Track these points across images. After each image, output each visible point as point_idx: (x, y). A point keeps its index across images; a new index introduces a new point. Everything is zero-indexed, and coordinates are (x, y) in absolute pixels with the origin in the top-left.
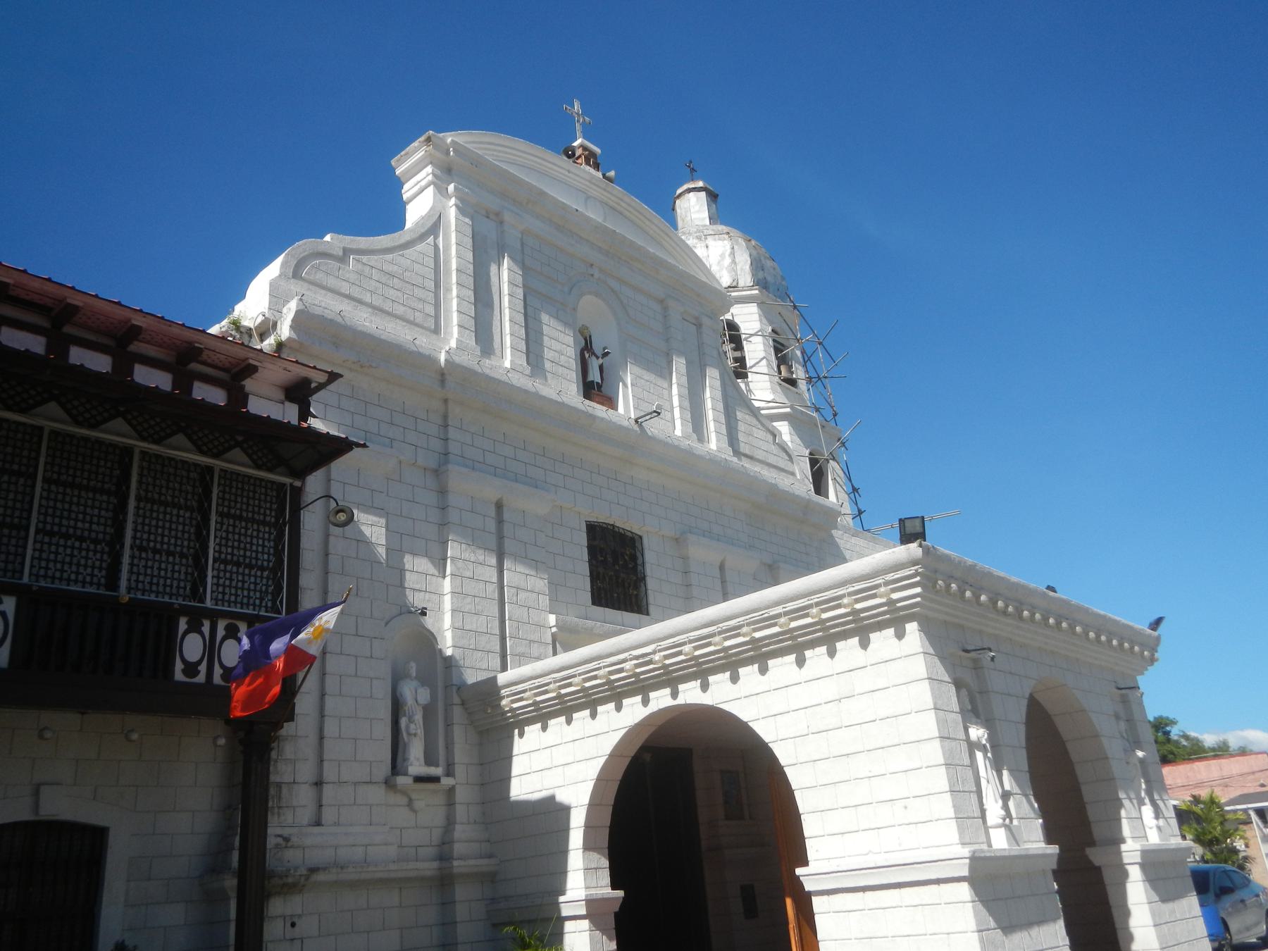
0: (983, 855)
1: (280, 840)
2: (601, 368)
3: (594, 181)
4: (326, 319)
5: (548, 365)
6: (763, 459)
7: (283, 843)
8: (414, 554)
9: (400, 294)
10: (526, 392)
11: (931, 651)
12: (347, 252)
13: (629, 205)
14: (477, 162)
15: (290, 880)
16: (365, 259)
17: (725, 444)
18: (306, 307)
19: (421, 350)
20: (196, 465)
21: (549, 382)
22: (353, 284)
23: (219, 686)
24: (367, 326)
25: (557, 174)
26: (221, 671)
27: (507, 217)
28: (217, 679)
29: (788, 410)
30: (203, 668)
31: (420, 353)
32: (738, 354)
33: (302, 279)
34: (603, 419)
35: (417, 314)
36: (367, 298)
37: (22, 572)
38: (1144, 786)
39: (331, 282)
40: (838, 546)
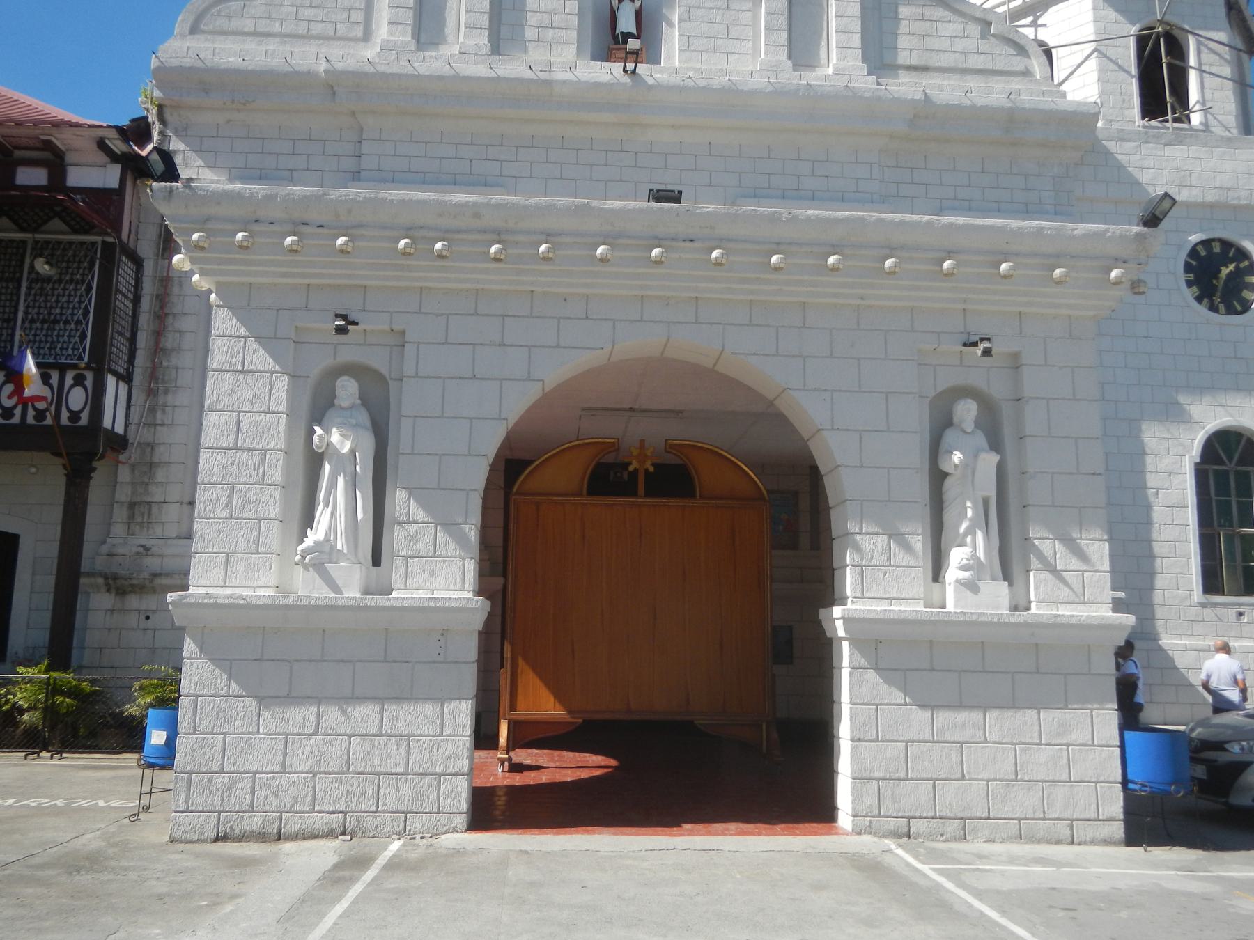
0: (211, 601)
1: (141, 549)
2: (639, 14)
4: (185, 68)
5: (530, 33)
6: (952, 65)
7: (144, 553)
9: (318, 11)
10: (441, 78)
11: (243, 331)
15: (135, 582)
17: (855, 62)
18: (162, 63)
19: (297, 68)
20: (12, 241)
21: (531, 53)
22: (258, 18)
23: (31, 426)
24: (231, 62)
26: (68, 414)
28: (30, 420)
30: (18, 411)
31: (297, 73)
33: (203, 32)
34: (564, 82)
36: (276, 28)
38: (970, 513)
39: (236, 24)
40: (1120, 167)
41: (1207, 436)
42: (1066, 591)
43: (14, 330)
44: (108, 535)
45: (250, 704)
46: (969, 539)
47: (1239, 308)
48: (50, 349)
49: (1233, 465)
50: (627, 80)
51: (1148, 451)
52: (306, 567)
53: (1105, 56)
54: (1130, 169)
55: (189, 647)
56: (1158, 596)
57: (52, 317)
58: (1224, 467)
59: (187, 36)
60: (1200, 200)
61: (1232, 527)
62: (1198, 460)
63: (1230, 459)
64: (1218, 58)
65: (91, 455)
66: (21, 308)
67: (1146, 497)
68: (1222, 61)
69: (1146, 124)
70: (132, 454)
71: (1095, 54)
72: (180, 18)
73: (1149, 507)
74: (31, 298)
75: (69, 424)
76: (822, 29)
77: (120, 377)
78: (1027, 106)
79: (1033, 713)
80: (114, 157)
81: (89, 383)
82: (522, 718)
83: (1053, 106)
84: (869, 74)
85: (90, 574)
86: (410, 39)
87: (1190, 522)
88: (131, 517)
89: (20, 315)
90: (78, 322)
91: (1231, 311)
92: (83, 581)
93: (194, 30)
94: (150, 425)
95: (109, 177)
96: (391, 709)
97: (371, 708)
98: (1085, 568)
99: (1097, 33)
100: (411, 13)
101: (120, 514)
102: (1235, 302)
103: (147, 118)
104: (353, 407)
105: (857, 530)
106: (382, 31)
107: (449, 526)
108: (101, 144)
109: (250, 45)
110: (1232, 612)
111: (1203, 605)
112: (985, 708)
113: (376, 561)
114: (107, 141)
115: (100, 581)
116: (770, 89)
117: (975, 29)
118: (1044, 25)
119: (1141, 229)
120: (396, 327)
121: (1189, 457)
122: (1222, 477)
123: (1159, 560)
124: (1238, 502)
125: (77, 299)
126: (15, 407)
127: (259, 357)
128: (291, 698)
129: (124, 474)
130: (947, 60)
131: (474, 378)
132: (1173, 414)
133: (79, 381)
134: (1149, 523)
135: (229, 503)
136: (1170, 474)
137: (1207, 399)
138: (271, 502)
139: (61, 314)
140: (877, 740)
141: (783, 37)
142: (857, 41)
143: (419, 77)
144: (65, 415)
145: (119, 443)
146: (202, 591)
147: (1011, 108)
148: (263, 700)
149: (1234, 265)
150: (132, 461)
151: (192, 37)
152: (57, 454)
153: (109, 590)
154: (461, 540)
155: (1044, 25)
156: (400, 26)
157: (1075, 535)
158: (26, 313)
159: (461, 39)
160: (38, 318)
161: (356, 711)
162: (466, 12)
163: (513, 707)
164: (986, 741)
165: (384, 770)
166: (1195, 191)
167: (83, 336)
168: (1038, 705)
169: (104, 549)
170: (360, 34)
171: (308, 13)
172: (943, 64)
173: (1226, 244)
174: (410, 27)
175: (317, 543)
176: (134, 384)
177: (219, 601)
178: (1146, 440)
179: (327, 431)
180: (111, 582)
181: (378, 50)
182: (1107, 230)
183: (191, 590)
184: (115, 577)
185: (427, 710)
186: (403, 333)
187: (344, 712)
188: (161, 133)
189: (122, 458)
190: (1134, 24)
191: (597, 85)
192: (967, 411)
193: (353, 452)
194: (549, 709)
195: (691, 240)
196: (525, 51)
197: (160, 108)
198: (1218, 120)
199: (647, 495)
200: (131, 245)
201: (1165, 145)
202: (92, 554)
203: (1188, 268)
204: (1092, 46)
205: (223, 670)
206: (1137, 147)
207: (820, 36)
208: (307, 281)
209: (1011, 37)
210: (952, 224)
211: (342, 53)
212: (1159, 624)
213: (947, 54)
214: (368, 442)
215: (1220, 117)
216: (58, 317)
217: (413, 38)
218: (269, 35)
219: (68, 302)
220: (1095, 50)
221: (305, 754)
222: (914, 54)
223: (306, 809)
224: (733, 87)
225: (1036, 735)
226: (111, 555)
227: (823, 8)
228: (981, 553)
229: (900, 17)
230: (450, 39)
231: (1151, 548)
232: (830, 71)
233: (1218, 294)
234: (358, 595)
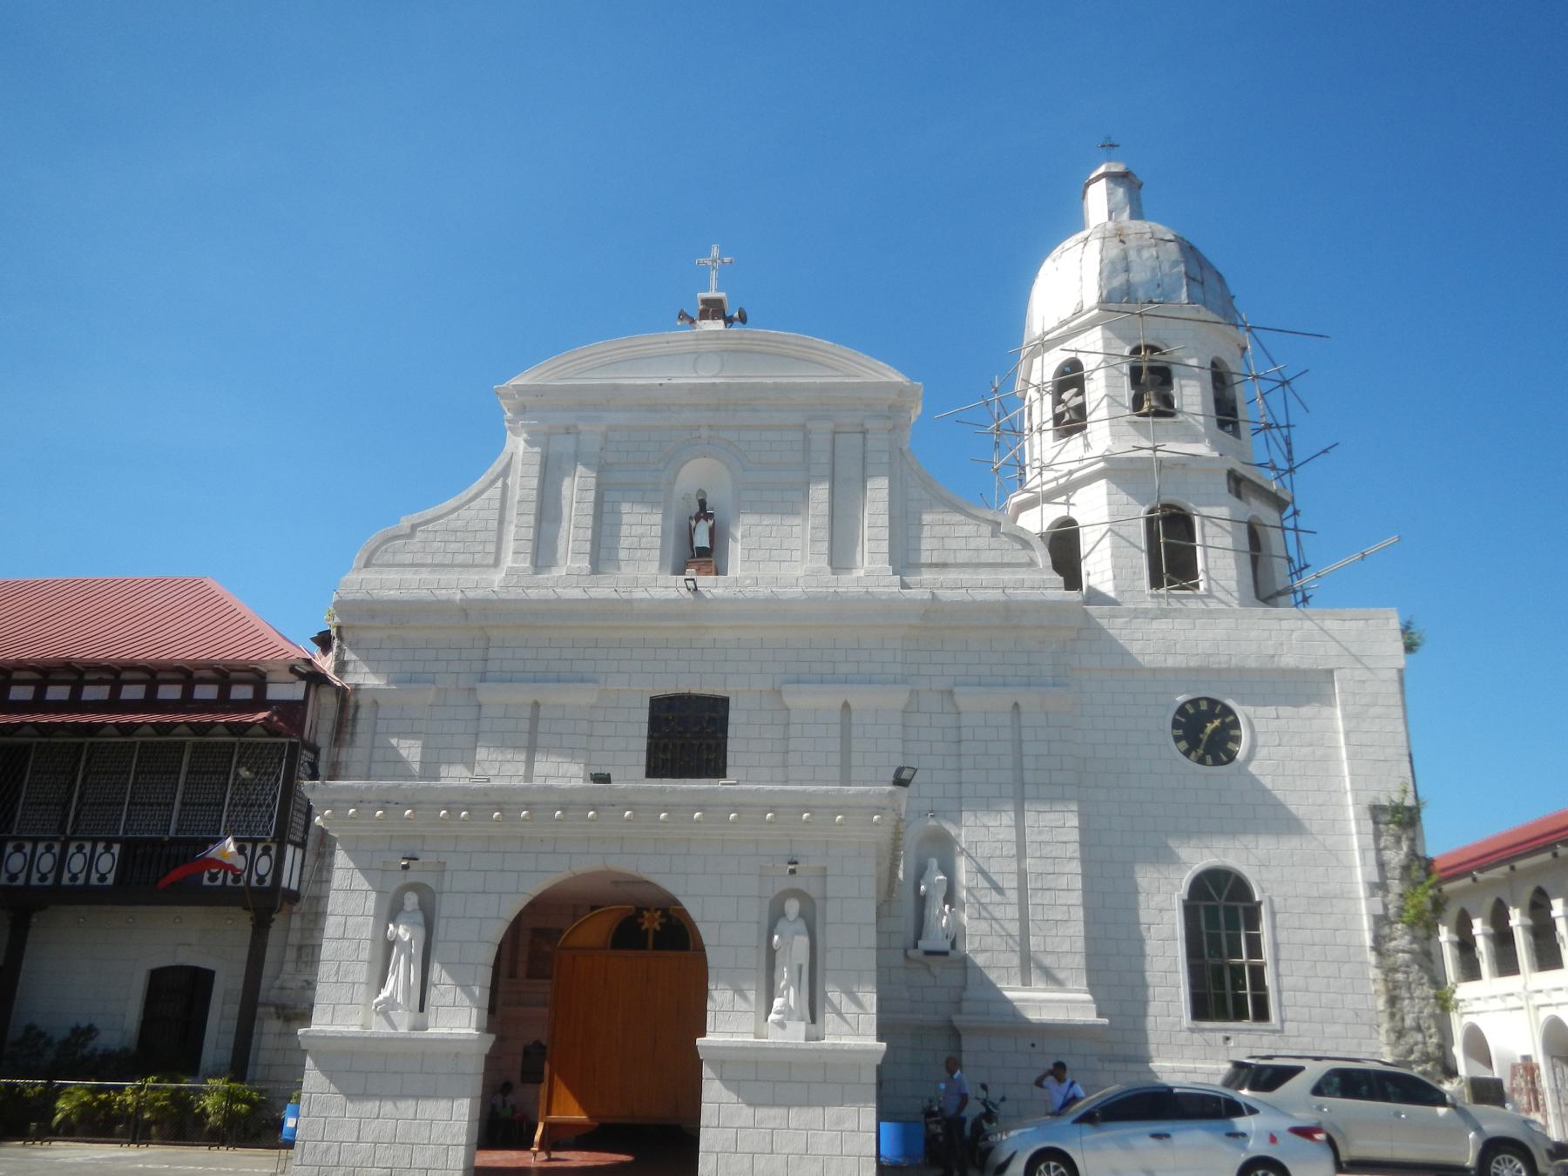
1: (305, 984)
2: (712, 531)
3: (701, 337)
5: (623, 554)
6: (967, 561)
8: (450, 763)
9: (461, 545)
10: (547, 601)
11: (352, 865)
12: (414, 527)
13: (754, 339)
14: (539, 392)
15: (298, 1011)
16: (430, 527)
17: (883, 565)
20: (225, 743)
25: (663, 350)
27: (581, 426)
28: (229, 882)
29: (1101, 465)
30: (221, 875)
31: (439, 601)
32: (1079, 400)
33: (374, 565)
34: (641, 600)
35: (477, 556)
37: (118, 830)
39: (399, 558)
41: (1193, 876)
42: (846, 1027)
43: (222, 812)
44: (281, 970)
45: (340, 1098)
46: (785, 992)
47: (1225, 759)
48: (247, 826)
49: (1222, 901)
50: (690, 596)
51: (1140, 889)
52: (378, 1014)
53: (1118, 535)
54: (1121, 642)
55: (309, 1062)
56: (1150, 1022)
57: (250, 802)
58: (1213, 903)
59: (361, 569)
60: (1184, 665)
61: (1221, 956)
62: (1186, 897)
63: (1220, 894)
64: (1220, 530)
65: (272, 910)
66: (228, 795)
67: (1140, 932)
68: (1224, 533)
69: (1155, 592)
70: (303, 905)
71: (1109, 534)
72: (358, 555)
73: (1141, 941)
74: (236, 787)
75: (257, 885)
76: (858, 536)
77: (296, 845)
78: (1019, 598)
79: (821, 1109)
80: (302, 676)
81: (273, 852)
82: (553, 1121)
83: (1042, 597)
84: (894, 574)
85: (265, 1005)
86: (528, 565)
87: (1179, 954)
88: (299, 957)
89: (227, 800)
90: (269, 806)
91: (1217, 762)
92: (260, 1010)
93: (368, 564)
94: (317, 882)
95: (296, 691)
96: (422, 1104)
97: (411, 1103)
98: (860, 1012)
99: (1111, 515)
100: (530, 544)
101: (291, 954)
103: (330, 631)
104: (413, 911)
105: (714, 987)
106: (508, 560)
107: (465, 988)
108: (292, 670)
109: (409, 576)
110: (1220, 1036)
111: (1192, 1030)
112: (789, 1106)
113: (422, 1009)
114: (296, 667)
115: (272, 1010)
116: (804, 597)
117: (986, 530)
118: (1073, 505)
119: (890, 788)
120: (442, 861)
121: (1178, 895)
122: (1212, 913)
123: (1151, 990)
124: (1227, 934)
125: (269, 787)
126: (219, 872)
127: (360, 882)
128: (365, 1096)
129: (296, 922)
130: (962, 557)
131: (484, 892)
132: (1164, 857)
133: (266, 851)
134: (1142, 955)
135: (337, 973)
136: (1161, 911)
137: (1194, 842)
138: (361, 972)
139: (257, 799)
140: (718, 1127)
141: (824, 547)
142: (885, 546)
143: (530, 601)
144: (254, 878)
145: (293, 897)
146: (318, 1028)
148: (351, 1096)
149: (1219, 721)
150: (301, 912)
151: (365, 569)
152: (246, 909)
153: (278, 1018)
154: (470, 995)
155: (1073, 505)
156: (523, 555)
157: (855, 989)
158: (231, 799)
159: (568, 564)
160: (240, 803)
161: (402, 1105)
162: (573, 541)
163: (549, 1113)
164: (788, 1128)
165: (416, 1141)
166: (1179, 658)
167: (271, 817)
168: (824, 1104)
169: (278, 983)
170: (491, 560)
171: (453, 547)
172: (959, 560)
173: (1213, 703)
174: (529, 555)
175: (385, 998)
176: (308, 847)
177: (328, 1034)
178: (1139, 880)
179: (396, 927)
180: (280, 1011)
181: (504, 575)
182: (870, 790)
183: (312, 1027)
184: (284, 1007)
185: (443, 1104)
186: (444, 863)
187: (395, 1105)
188: (339, 647)
189: (295, 909)
190: (1144, 505)
191: (667, 601)
192: (792, 907)
193: (411, 940)
194: (571, 1112)
195: (613, 805)
196: (619, 568)
197: (339, 628)
198: (1220, 586)
199: (655, 948)
200: (311, 741)
201: (1152, 619)
202: (268, 989)
204: (1106, 527)
205: (328, 1078)
206: (1127, 622)
207: (857, 545)
208: (390, 834)
209: (1017, 534)
210: (771, 791)
211: (477, 577)
212: (1152, 1048)
213: (962, 552)
214: (421, 933)
215: (1222, 583)
216: (254, 802)
217: (532, 563)
218: (423, 565)
219: (262, 790)
220: (1109, 530)
221: (371, 1130)
222: (935, 553)
223: (369, 1165)
224: (775, 597)
225: (822, 1124)
226: (282, 988)
227: (860, 520)
228: (792, 1002)
229: (924, 523)
230: (561, 562)
231: (1143, 978)
232: (861, 573)
233: (1202, 747)
234: (406, 1031)
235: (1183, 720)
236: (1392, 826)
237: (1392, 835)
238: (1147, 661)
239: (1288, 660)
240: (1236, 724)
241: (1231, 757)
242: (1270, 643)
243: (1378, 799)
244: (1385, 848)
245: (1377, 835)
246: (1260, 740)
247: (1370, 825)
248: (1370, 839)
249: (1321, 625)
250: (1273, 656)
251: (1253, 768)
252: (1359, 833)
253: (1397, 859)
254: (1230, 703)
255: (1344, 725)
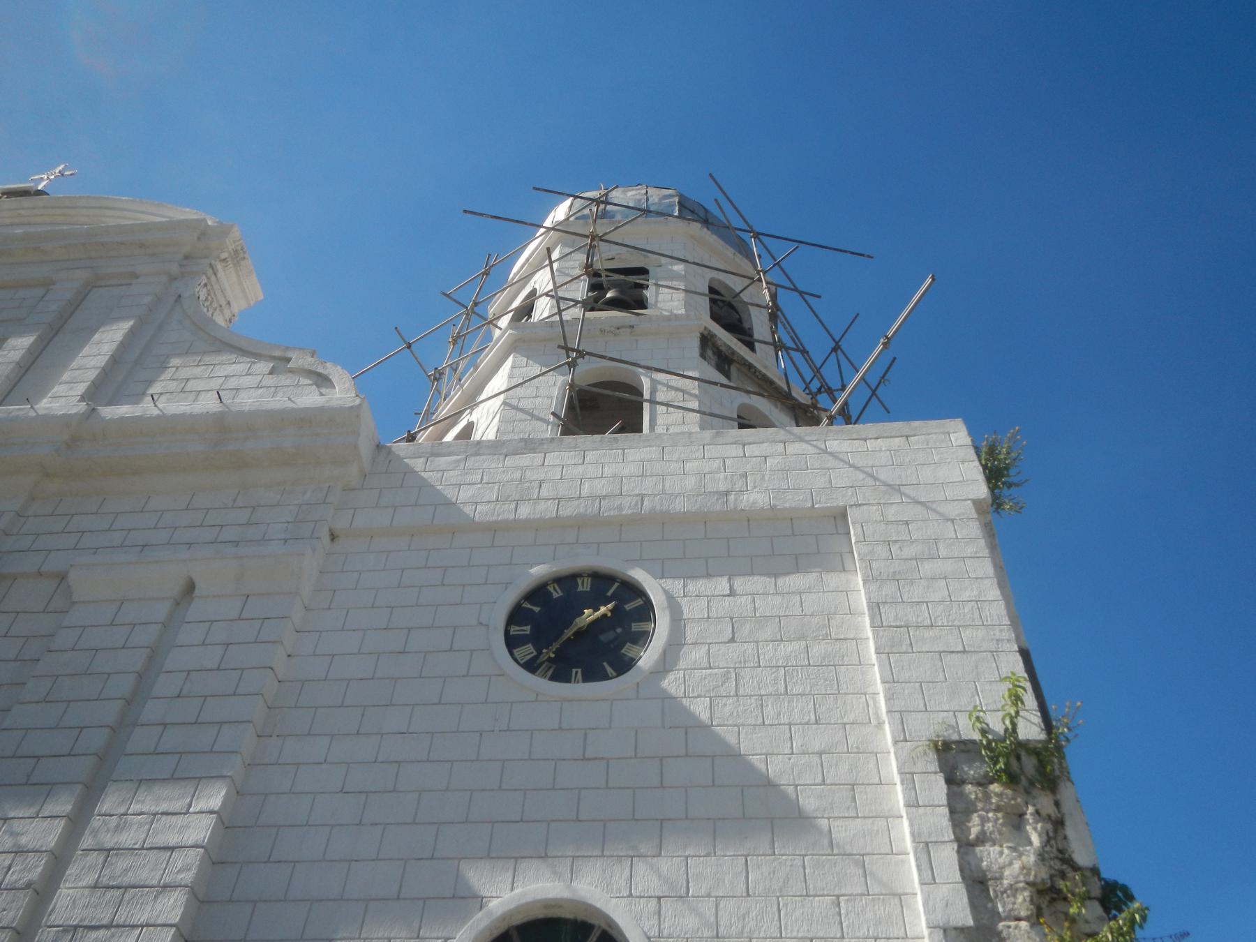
40: (425, 485)
102: (605, 664)
147: (222, 413)
166: (542, 506)
203: (516, 615)
206: (459, 461)
209: (313, 368)
220: (504, 403)
235: (537, 609)
236: (995, 788)
237: (998, 809)
238: (482, 513)
239: (756, 498)
240: (646, 611)
241: (624, 666)
242: (722, 476)
243: (956, 728)
244: (982, 839)
245: (959, 811)
246: (691, 634)
247: (938, 789)
248: (941, 819)
249: (823, 446)
250: (727, 493)
251: (671, 683)
252: (912, 804)
253: (1017, 865)
254: (640, 575)
255: (868, 593)
